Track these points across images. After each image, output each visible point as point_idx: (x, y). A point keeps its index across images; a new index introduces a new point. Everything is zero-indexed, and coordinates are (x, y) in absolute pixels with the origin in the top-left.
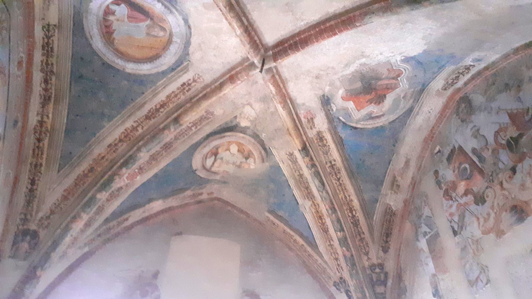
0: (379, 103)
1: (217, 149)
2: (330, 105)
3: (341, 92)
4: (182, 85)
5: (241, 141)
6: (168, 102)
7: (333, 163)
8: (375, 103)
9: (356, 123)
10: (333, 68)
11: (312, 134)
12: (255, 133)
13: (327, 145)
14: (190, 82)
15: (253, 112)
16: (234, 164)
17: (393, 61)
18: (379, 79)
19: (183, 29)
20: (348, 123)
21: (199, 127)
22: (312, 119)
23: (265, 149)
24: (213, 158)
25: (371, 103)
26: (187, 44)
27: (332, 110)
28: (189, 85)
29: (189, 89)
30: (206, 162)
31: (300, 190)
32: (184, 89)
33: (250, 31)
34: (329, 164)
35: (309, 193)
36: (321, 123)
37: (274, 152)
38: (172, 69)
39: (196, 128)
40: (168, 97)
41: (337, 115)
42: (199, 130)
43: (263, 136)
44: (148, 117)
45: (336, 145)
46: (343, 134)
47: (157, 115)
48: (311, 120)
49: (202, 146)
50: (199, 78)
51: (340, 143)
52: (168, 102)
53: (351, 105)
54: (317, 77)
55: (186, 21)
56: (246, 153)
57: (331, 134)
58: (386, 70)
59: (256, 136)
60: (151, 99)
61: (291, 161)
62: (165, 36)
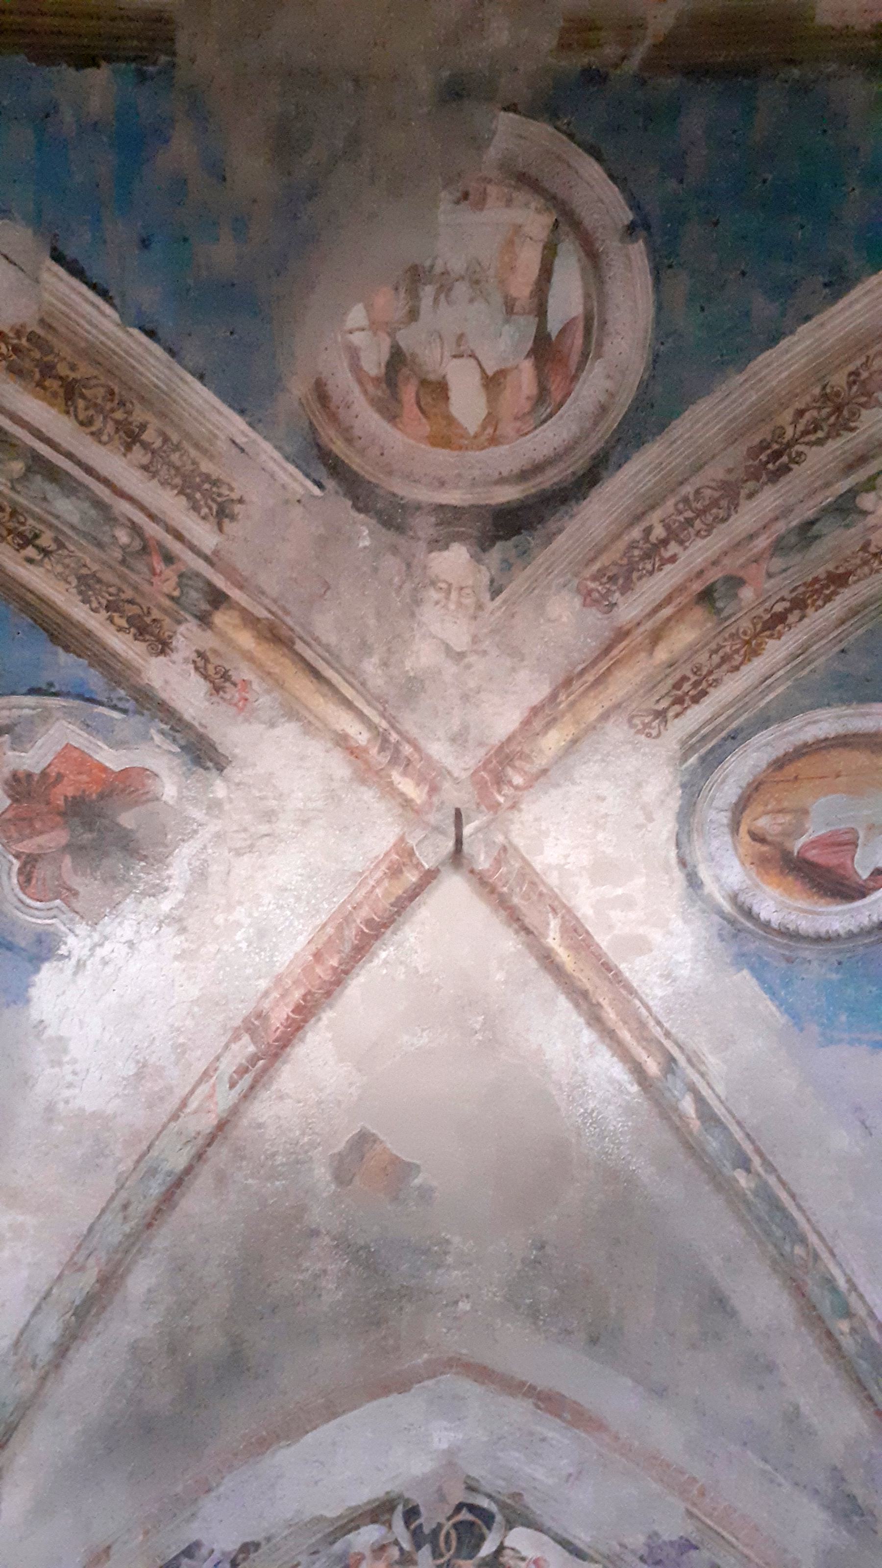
1: (542, 395)
2: (181, 747)
3: (169, 790)
4: (704, 693)
5: (443, 455)
6: (756, 636)
7: (30, 551)
8: (29, 775)
10: (239, 853)
12: (400, 529)
13: (104, 614)
14: (677, 708)
15: (436, 628)
16: (445, 289)
17: (82, 928)
18: (74, 849)
19: (698, 853)
20: (77, 703)
21: (636, 533)
22: (217, 689)
24: (554, 326)
25: (44, 774)
26: (687, 815)
27: (162, 732)
28: (679, 701)
29: (677, 686)
30: (587, 296)
31: (92, 353)
32: (696, 684)
33: (513, 898)
34: (46, 541)
35: (47, 370)
36: (173, 677)
37: (296, 482)
38: (737, 738)
39: (648, 531)
40: (755, 652)
42: (638, 518)
43: (365, 534)
45: (66, 618)
46: (66, 665)
47: (802, 589)
48: (219, 681)
50: (646, 726)
51: (58, 632)
52: (756, 636)
53: (112, 759)
54: (269, 816)
55: (693, 882)
56: (409, 393)
57: (114, 655)
58: (81, 889)
59: (393, 516)
60: (818, 636)
61: (207, 478)
62: (755, 819)
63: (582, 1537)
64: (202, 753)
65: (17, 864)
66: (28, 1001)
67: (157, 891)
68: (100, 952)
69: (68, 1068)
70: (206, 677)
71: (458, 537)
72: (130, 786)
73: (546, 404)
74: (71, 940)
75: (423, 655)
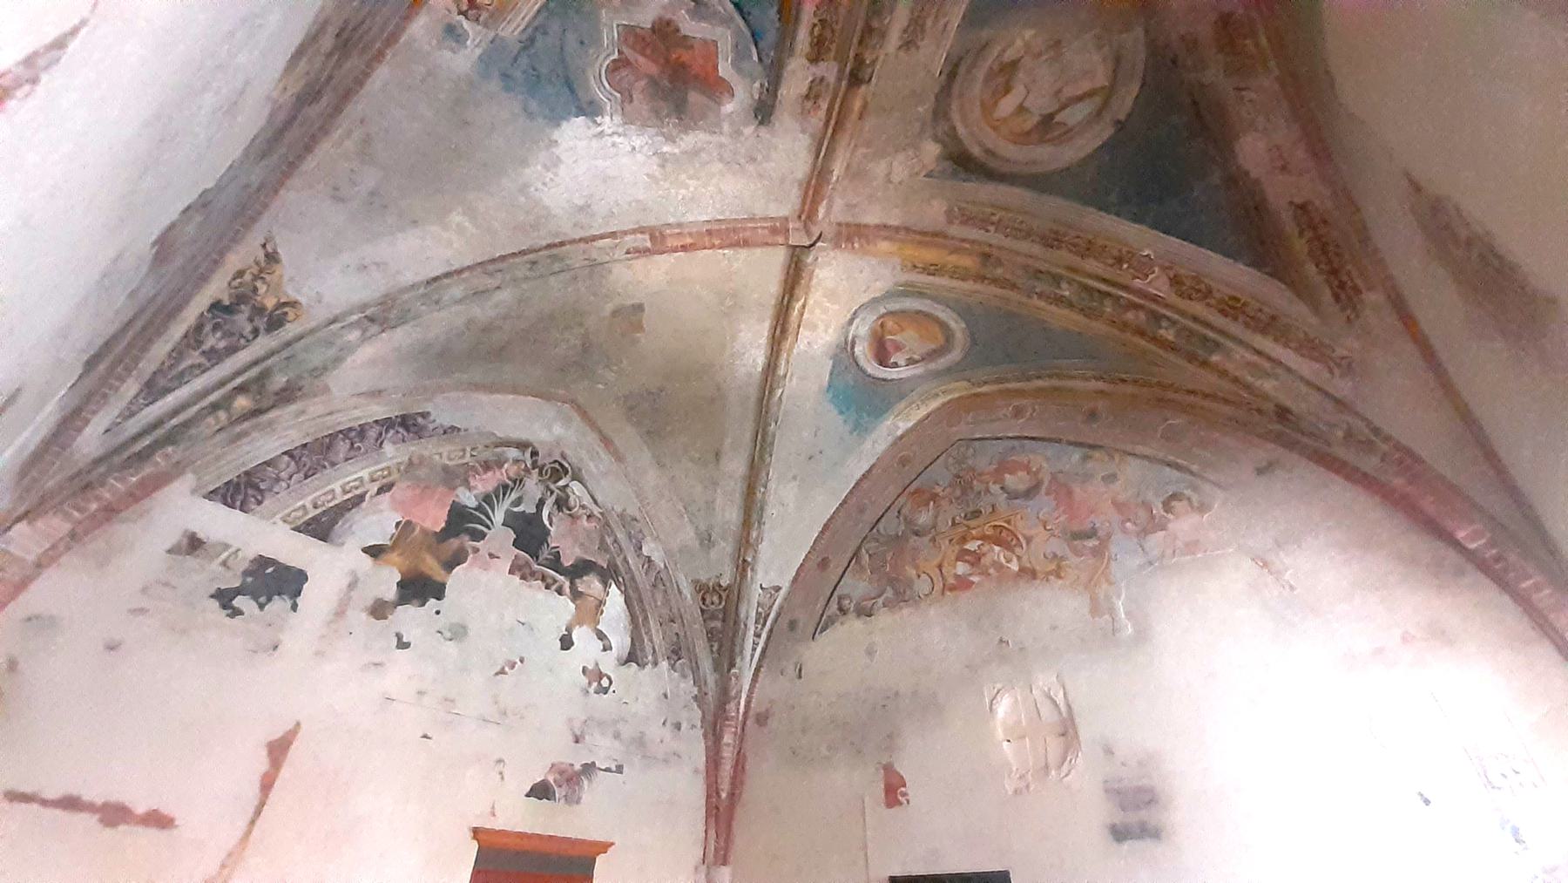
0: (669, 23)
3: (729, 107)
8: (678, 30)
9: (732, 18)
10: (721, 159)
11: (828, 70)
15: (895, 164)
17: (618, 119)
18: (653, 82)
21: (989, 210)
22: (807, 97)
23: (952, 76)
41: (760, 68)
44: (1014, 286)
48: (812, 96)
49: (1034, 170)
53: (725, 69)
54: (753, 160)
58: (636, 102)
59: (940, 112)
63: (600, 499)
64: (764, 112)
65: (616, 56)
66: (559, 125)
67: (670, 139)
68: (616, 139)
69: (550, 175)
70: (810, 88)
71: (945, 146)
72: (716, 88)
73: (1023, 138)
74: (607, 118)
75: (880, 168)
